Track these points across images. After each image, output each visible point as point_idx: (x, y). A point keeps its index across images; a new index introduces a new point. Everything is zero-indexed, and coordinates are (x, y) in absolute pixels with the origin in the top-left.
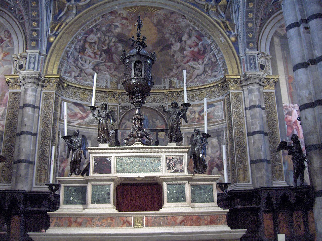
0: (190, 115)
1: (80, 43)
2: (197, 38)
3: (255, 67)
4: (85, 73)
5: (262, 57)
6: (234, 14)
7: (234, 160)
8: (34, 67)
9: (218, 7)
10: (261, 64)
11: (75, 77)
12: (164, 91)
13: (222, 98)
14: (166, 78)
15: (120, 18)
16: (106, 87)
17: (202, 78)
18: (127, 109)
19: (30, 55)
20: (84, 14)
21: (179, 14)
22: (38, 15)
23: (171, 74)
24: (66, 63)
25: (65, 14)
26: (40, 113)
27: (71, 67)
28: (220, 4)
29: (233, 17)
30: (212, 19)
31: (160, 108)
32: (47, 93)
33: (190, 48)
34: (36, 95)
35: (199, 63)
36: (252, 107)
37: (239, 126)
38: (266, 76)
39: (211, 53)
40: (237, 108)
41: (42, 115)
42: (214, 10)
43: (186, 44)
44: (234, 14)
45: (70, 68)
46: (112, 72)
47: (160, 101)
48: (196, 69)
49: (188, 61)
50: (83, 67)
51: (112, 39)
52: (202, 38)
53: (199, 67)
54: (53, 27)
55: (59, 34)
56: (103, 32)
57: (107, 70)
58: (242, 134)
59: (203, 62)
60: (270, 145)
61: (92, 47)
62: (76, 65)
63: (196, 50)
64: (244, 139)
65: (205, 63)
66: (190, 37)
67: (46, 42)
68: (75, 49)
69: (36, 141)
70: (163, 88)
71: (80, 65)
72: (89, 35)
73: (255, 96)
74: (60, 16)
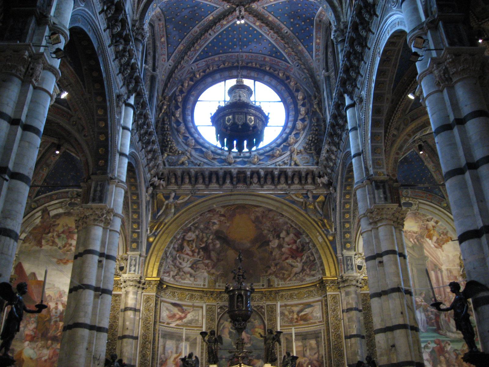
0: (289, 315)
1: (178, 242)
2: (295, 235)
3: (352, 269)
4: (183, 271)
5: (360, 257)
6: (332, 211)
7: (332, 363)
8: (135, 269)
9: (316, 204)
10: (358, 264)
11: (173, 277)
12: (262, 290)
13: (319, 298)
14: (265, 276)
15: (218, 215)
16: (204, 285)
17: (301, 277)
18: (225, 308)
19: (131, 257)
20: (183, 213)
21: (277, 212)
22: (139, 217)
23: (269, 272)
24: (164, 263)
25: (162, 213)
26: (141, 315)
27: (170, 266)
28: (318, 200)
29: (331, 214)
30: (310, 217)
31: (258, 308)
32: (147, 295)
33: (289, 245)
34: (136, 298)
35: (297, 261)
36: (349, 310)
37: (337, 328)
38: (364, 277)
39: (309, 252)
40: (334, 310)
41: (143, 318)
42: (311, 207)
43: (284, 241)
44: (332, 211)
45: (168, 267)
46: (209, 270)
47: (258, 300)
48: (295, 267)
49: (286, 259)
50: (181, 266)
51: (210, 236)
52: (301, 236)
53: (297, 265)
54: (152, 226)
55: (158, 234)
56: (200, 230)
57: (205, 268)
58: (339, 337)
59: (301, 260)
60: (368, 348)
61: (190, 245)
62: (174, 264)
63: (294, 247)
64: (341, 342)
65: (303, 261)
66: (288, 234)
67: (146, 243)
68: (174, 248)
69: (137, 344)
70: (262, 287)
71: (178, 264)
72: (187, 233)
73: (352, 298)
74: (159, 214)
